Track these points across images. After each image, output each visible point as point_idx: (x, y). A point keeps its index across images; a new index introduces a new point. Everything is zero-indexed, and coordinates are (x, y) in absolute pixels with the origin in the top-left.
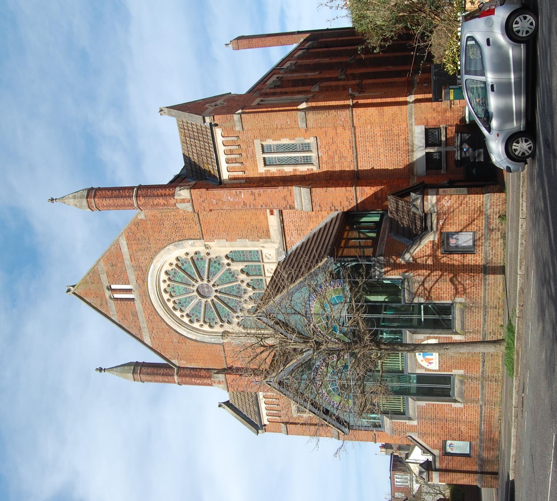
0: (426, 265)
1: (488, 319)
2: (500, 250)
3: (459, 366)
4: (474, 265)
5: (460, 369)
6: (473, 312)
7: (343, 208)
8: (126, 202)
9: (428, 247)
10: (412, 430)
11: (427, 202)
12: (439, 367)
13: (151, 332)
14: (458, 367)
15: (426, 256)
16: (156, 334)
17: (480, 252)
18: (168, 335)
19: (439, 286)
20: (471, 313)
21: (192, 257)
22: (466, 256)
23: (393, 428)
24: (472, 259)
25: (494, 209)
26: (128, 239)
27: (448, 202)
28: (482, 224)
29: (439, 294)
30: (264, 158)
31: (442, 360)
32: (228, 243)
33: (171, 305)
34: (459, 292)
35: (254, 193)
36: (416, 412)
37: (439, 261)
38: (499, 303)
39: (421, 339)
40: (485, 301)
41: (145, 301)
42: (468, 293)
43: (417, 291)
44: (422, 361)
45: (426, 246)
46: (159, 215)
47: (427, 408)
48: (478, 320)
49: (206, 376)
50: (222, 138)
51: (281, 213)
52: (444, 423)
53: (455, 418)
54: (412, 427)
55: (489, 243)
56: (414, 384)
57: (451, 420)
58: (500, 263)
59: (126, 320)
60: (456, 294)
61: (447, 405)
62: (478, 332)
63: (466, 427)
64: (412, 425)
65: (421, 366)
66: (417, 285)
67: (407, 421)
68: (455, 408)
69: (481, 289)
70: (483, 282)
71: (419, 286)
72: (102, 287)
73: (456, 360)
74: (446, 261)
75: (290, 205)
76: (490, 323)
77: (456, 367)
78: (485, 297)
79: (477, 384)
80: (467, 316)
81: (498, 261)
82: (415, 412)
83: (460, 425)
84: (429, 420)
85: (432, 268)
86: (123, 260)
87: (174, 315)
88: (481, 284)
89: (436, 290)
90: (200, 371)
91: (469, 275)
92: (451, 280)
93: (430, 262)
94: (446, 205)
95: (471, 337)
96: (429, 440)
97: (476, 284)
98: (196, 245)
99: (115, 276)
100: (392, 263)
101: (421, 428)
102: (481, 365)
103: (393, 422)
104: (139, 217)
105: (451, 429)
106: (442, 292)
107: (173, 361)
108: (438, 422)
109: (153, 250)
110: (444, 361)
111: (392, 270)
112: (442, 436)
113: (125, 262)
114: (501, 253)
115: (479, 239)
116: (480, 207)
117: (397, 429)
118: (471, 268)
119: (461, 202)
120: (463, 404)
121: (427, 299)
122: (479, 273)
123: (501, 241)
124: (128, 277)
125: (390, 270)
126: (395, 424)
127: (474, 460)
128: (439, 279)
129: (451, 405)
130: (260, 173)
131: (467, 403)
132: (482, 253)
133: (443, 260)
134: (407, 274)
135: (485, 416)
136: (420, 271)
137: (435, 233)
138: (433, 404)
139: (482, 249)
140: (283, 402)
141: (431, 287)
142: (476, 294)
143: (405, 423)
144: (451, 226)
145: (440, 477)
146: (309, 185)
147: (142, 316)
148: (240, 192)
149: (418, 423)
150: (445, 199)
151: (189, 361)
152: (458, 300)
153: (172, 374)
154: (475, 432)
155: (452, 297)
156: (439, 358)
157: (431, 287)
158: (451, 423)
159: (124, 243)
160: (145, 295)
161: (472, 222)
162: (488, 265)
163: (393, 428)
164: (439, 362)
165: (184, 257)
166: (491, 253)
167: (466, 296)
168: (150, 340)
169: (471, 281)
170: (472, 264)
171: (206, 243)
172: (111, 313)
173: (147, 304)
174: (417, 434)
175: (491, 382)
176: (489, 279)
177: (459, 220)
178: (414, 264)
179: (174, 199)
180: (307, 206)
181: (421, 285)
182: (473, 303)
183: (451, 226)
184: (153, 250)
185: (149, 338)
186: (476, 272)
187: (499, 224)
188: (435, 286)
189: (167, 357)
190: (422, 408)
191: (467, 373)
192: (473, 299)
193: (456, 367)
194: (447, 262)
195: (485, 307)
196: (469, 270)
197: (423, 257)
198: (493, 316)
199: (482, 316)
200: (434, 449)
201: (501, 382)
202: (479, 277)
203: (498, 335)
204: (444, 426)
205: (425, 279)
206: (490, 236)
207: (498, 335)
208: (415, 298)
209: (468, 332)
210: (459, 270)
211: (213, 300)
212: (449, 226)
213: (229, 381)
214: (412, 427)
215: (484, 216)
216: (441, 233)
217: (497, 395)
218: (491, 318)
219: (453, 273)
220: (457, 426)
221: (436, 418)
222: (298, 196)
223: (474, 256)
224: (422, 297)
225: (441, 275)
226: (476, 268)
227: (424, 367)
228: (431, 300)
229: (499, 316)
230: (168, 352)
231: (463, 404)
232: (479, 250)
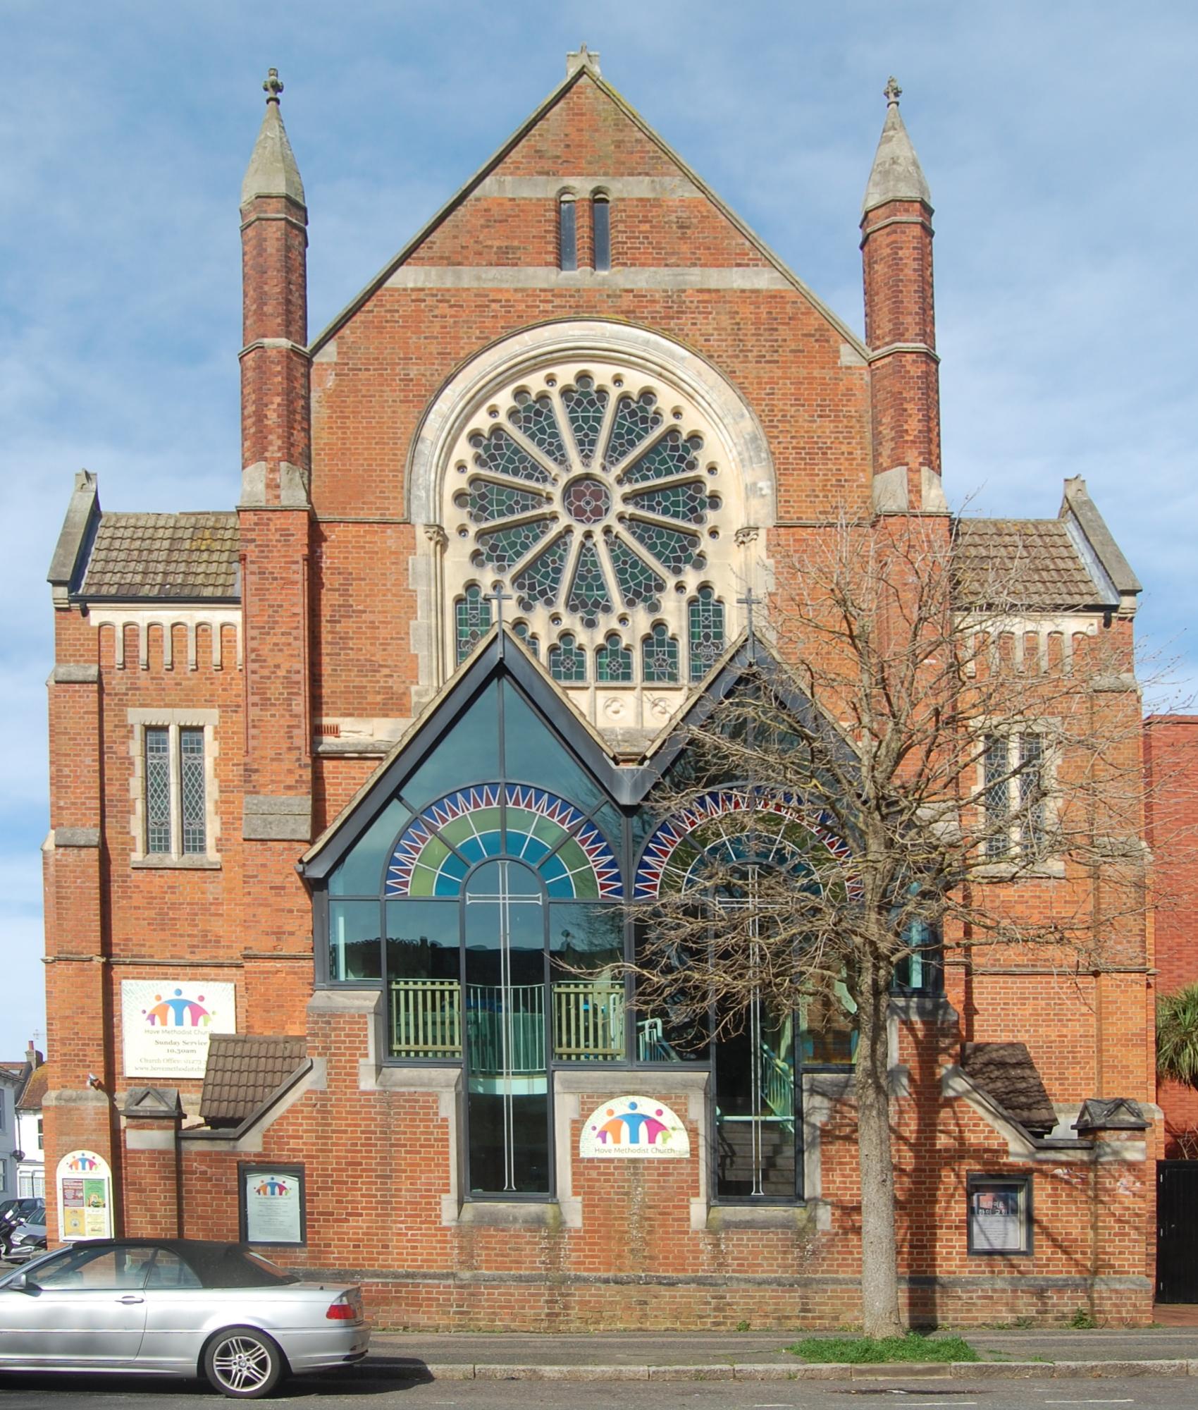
1: (768, 1293)
4: (934, 1253)
5: (584, 1218)
12: (591, 1160)
13: (442, 296)
16: (436, 312)
18: (435, 352)
25: (1110, 1299)
28: (1053, 1272)
31: (615, 1168)
33: (535, 382)
36: (412, 1089)
40: (819, 1281)
41: (557, 302)
42: (846, 1240)
46: (853, 409)
47: (432, 1120)
48: (760, 1265)
50: (1071, 632)
55: (1004, 1291)
56: (512, 1086)
59: (482, 221)
61: (448, 1178)
62: (720, 1265)
64: (357, 1075)
67: (372, 1059)
73: (618, 1207)
76: (752, 1297)
80: (771, 1236)
82: (412, 1085)
84: (382, 1126)
87: (501, 386)
91: (904, 1240)
95: (701, 1246)
96: (301, 1125)
98: (755, 502)
101: (349, 1100)
108: (377, 1152)
109: (737, 366)
114: (976, 1319)
118: (925, 1247)
122: (909, 1266)
132: (970, 1272)
139: (984, 1272)
140: (184, 683)
142: (844, 1259)
143: (366, 1055)
147: (501, 281)
149: (364, 1093)
162: (938, 1288)
166: (974, 1295)
167: (837, 1234)
168: (411, 285)
171: (762, 533)
172: (509, 178)
173: (549, 307)
174: (322, 1086)
182: (814, 1252)
184: (737, 366)
185: (420, 285)
187: (1058, 1311)
190: (431, 1108)
191: (570, 1238)
199: (773, 1275)
206: (1023, 1291)
209: (719, 1239)
221: (392, 1145)
223: (962, 1253)
226: (926, 1259)
230: (367, 337)
232: (980, 1266)
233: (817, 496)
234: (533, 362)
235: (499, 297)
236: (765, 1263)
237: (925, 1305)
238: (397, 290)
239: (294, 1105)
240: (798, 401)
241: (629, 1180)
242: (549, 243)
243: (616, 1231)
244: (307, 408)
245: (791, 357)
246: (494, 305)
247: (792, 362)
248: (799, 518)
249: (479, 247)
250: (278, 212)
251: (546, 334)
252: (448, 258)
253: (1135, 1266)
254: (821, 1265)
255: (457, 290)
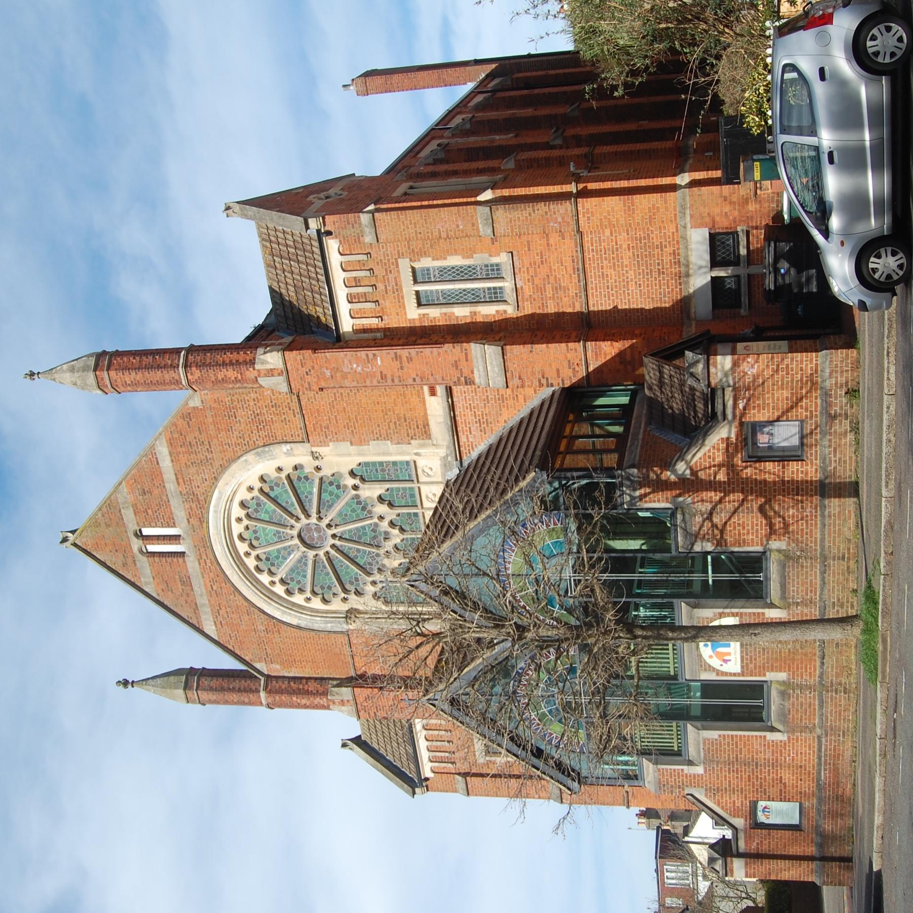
0: (715, 482)
1: (830, 578)
2: (849, 452)
3: (778, 665)
4: (802, 481)
6: (802, 567)
7: (563, 380)
8: (167, 377)
9: (718, 450)
10: (695, 783)
11: (716, 367)
12: (742, 667)
13: (216, 613)
14: (776, 667)
15: (714, 466)
16: (226, 616)
17: (814, 458)
19: (739, 520)
20: (798, 568)
21: (289, 475)
22: (788, 465)
23: (660, 780)
24: (798, 470)
25: (837, 378)
26: (171, 443)
27: (752, 367)
29: (739, 534)
30: (417, 293)
31: (747, 655)
32: (353, 449)
33: (251, 563)
34: (775, 531)
35: (400, 356)
36: (702, 750)
37: (738, 474)
38: (849, 549)
39: (707, 618)
42: (793, 532)
43: (700, 529)
44: (711, 657)
45: (714, 447)
46: (227, 399)
47: (721, 742)
48: (811, 581)
49: (317, 691)
50: (340, 257)
51: (449, 392)
52: (753, 770)
53: (773, 759)
54: (694, 778)
55: (830, 440)
57: (765, 764)
58: (850, 477)
59: (170, 593)
60: (771, 534)
61: (756, 736)
62: (811, 602)
63: (793, 776)
64: (694, 775)
65: (710, 666)
66: (698, 519)
67: (685, 767)
68: (773, 741)
69: (816, 524)
70: (819, 512)
71: (704, 521)
72: (126, 532)
74: (752, 475)
75: (465, 378)
76: (834, 587)
77: (772, 666)
78: (823, 540)
79: (810, 697)
80: (791, 574)
81: (846, 474)
82: (699, 750)
83: (781, 773)
84: (725, 765)
85: (725, 488)
86: (164, 483)
87: (258, 581)
88: (816, 516)
89: (735, 528)
90: (307, 683)
91: (793, 499)
92: (761, 509)
93: (722, 477)
94: (749, 373)
95: (799, 612)
96: (726, 801)
97: (807, 516)
98: (296, 452)
99: (150, 511)
100: (652, 480)
101: (710, 778)
102: (818, 664)
103: (659, 770)
104: (192, 404)
105: (765, 781)
106: (745, 532)
107: (258, 666)
108: (741, 767)
109: (217, 464)
110: (751, 657)
111: (653, 492)
112: (750, 794)
113: (167, 486)
114: (851, 458)
115: (811, 433)
116: (812, 374)
117: (668, 783)
118: (797, 487)
119: (778, 366)
120: (786, 734)
121: (717, 545)
122: (812, 496)
123: (850, 437)
124: (172, 513)
125: (649, 493)
126: (663, 773)
127: (808, 836)
128: (738, 508)
129: (765, 737)
130: (409, 320)
131: (793, 732)
132: (816, 459)
133: (747, 473)
134: (681, 499)
135: (826, 755)
136: (704, 493)
137: (730, 423)
138: (732, 736)
139: (816, 451)
140: (458, 736)
141: (726, 523)
142: (807, 534)
143: (682, 770)
144: (759, 411)
145: (746, 867)
146: (500, 340)
148: (374, 355)
149: (705, 771)
150: (748, 362)
151: (284, 664)
152: (775, 544)
153: (256, 689)
154: (809, 785)
155: (764, 539)
156: (742, 652)
157: (726, 523)
158: (765, 768)
159: (163, 451)
160: (204, 545)
161: (797, 404)
162: (827, 481)
163: (660, 780)
164: (742, 658)
165: (274, 474)
166: (833, 459)
167: (789, 538)
168: (214, 628)
169: (798, 510)
170: (799, 479)
171: (314, 449)
172: (142, 579)
173: (208, 561)
174: (703, 791)
175: (836, 693)
176: (830, 506)
177: (773, 398)
178: (693, 481)
179: (254, 369)
180: (496, 379)
181: (707, 518)
183: (759, 411)
184: (217, 464)
185: (213, 623)
186: (807, 494)
187: (846, 405)
188: (732, 520)
189: (247, 658)
190: (712, 742)
191: (793, 678)
192: (802, 542)
193: (772, 666)
194: (754, 477)
195: (824, 558)
196: (793, 489)
197: (710, 467)
198: (839, 574)
199: (818, 574)
200: (734, 817)
201: (854, 693)
202: (812, 503)
203: (847, 607)
204: (753, 774)
205: (713, 509)
206: (831, 429)
207: (847, 607)
208: (697, 543)
209: (794, 603)
210: (775, 491)
211: (327, 552)
212: (756, 411)
213: (360, 699)
214: (694, 778)
215: (819, 391)
216: (741, 424)
217: (849, 716)
218: (834, 577)
219: (765, 497)
220: (777, 775)
221: (737, 760)
222: (480, 360)
223: (802, 465)
224: (708, 539)
225: (743, 500)
226: (807, 487)
227: (714, 669)
228: (726, 545)
229: (849, 573)
231: (786, 734)
232: (811, 454)
233: (285, 419)
234: (240, 567)
235: (209, 585)
236: (809, 578)
237: (840, 489)
238: (218, 634)
239: (715, 803)
240: (229, 429)
241: (755, 649)
242: (172, 561)
243: (789, 655)
244: (294, 679)
245: (204, 435)
246: (215, 588)
247: (207, 434)
248: (301, 429)
249: (184, 595)
250: (193, 694)
251: (224, 563)
252: (194, 610)
253: (811, 360)
254: (811, 547)
255: (211, 606)
